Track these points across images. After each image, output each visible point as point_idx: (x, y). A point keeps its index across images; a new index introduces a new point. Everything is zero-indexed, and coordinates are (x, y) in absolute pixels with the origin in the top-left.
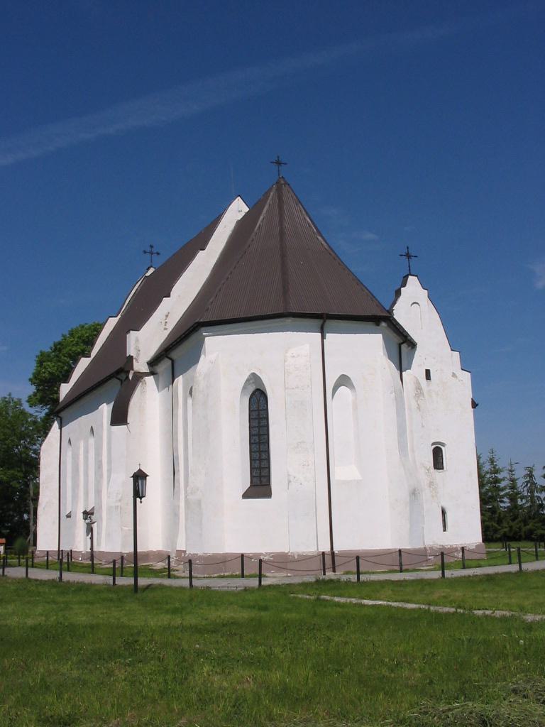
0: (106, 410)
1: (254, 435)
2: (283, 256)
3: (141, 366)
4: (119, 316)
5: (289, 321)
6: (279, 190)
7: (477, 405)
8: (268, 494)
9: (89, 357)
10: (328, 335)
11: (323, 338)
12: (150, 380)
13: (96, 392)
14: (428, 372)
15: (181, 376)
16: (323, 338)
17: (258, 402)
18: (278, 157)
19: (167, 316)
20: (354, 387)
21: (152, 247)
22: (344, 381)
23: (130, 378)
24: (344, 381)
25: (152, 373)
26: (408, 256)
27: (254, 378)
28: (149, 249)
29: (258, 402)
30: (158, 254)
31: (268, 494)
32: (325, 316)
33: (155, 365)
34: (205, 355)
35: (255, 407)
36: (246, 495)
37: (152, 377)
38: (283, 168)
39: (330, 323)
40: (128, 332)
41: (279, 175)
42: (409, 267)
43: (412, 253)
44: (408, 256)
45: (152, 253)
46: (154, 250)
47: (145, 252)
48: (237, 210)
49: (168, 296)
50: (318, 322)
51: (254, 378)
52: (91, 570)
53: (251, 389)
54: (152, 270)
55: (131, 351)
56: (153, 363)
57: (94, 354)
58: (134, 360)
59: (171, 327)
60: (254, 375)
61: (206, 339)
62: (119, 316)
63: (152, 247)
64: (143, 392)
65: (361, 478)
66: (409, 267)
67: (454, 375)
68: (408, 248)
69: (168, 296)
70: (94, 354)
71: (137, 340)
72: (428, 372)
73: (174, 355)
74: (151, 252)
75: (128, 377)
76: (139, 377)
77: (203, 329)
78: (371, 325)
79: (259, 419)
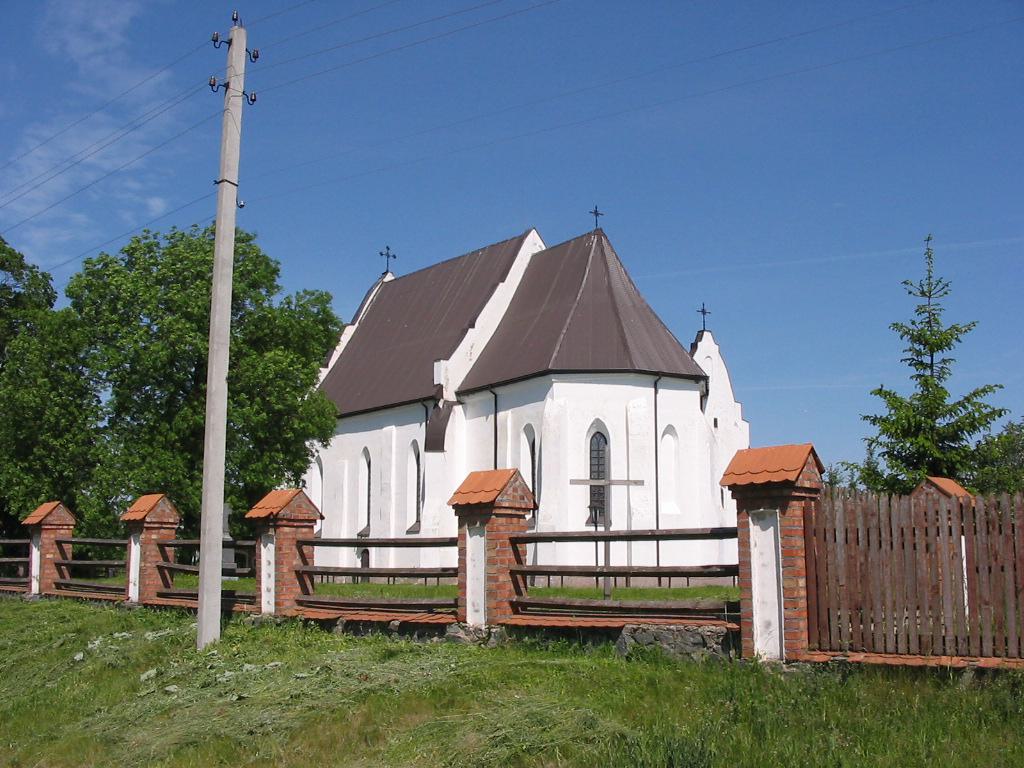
0: (418, 432)
2: (617, 314)
3: (449, 395)
4: (357, 324)
5: (632, 375)
6: (599, 242)
9: (326, 366)
10: (660, 391)
11: (656, 392)
12: (458, 409)
13: (388, 412)
14: (716, 420)
15: (509, 412)
16: (656, 392)
17: (599, 441)
20: (676, 435)
21: (388, 248)
22: (670, 430)
24: (670, 430)
25: (459, 402)
27: (598, 422)
28: (385, 251)
29: (599, 441)
30: (394, 257)
34: (552, 398)
35: (596, 448)
37: (460, 406)
38: (600, 218)
39: (664, 379)
40: (439, 360)
45: (388, 256)
48: (533, 245)
49: (473, 326)
50: (652, 379)
51: (598, 422)
53: (593, 432)
54: (389, 277)
56: (458, 394)
57: (331, 364)
60: (598, 420)
61: (554, 385)
62: (357, 324)
63: (388, 248)
64: (453, 421)
67: (736, 424)
70: (331, 364)
71: (447, 370)
72: (716, 420)
73: (499, 391)
74: (387, 254)
75: (436, 405)
76: (450, 406)
77: (552, 375)
78: (691, 383)
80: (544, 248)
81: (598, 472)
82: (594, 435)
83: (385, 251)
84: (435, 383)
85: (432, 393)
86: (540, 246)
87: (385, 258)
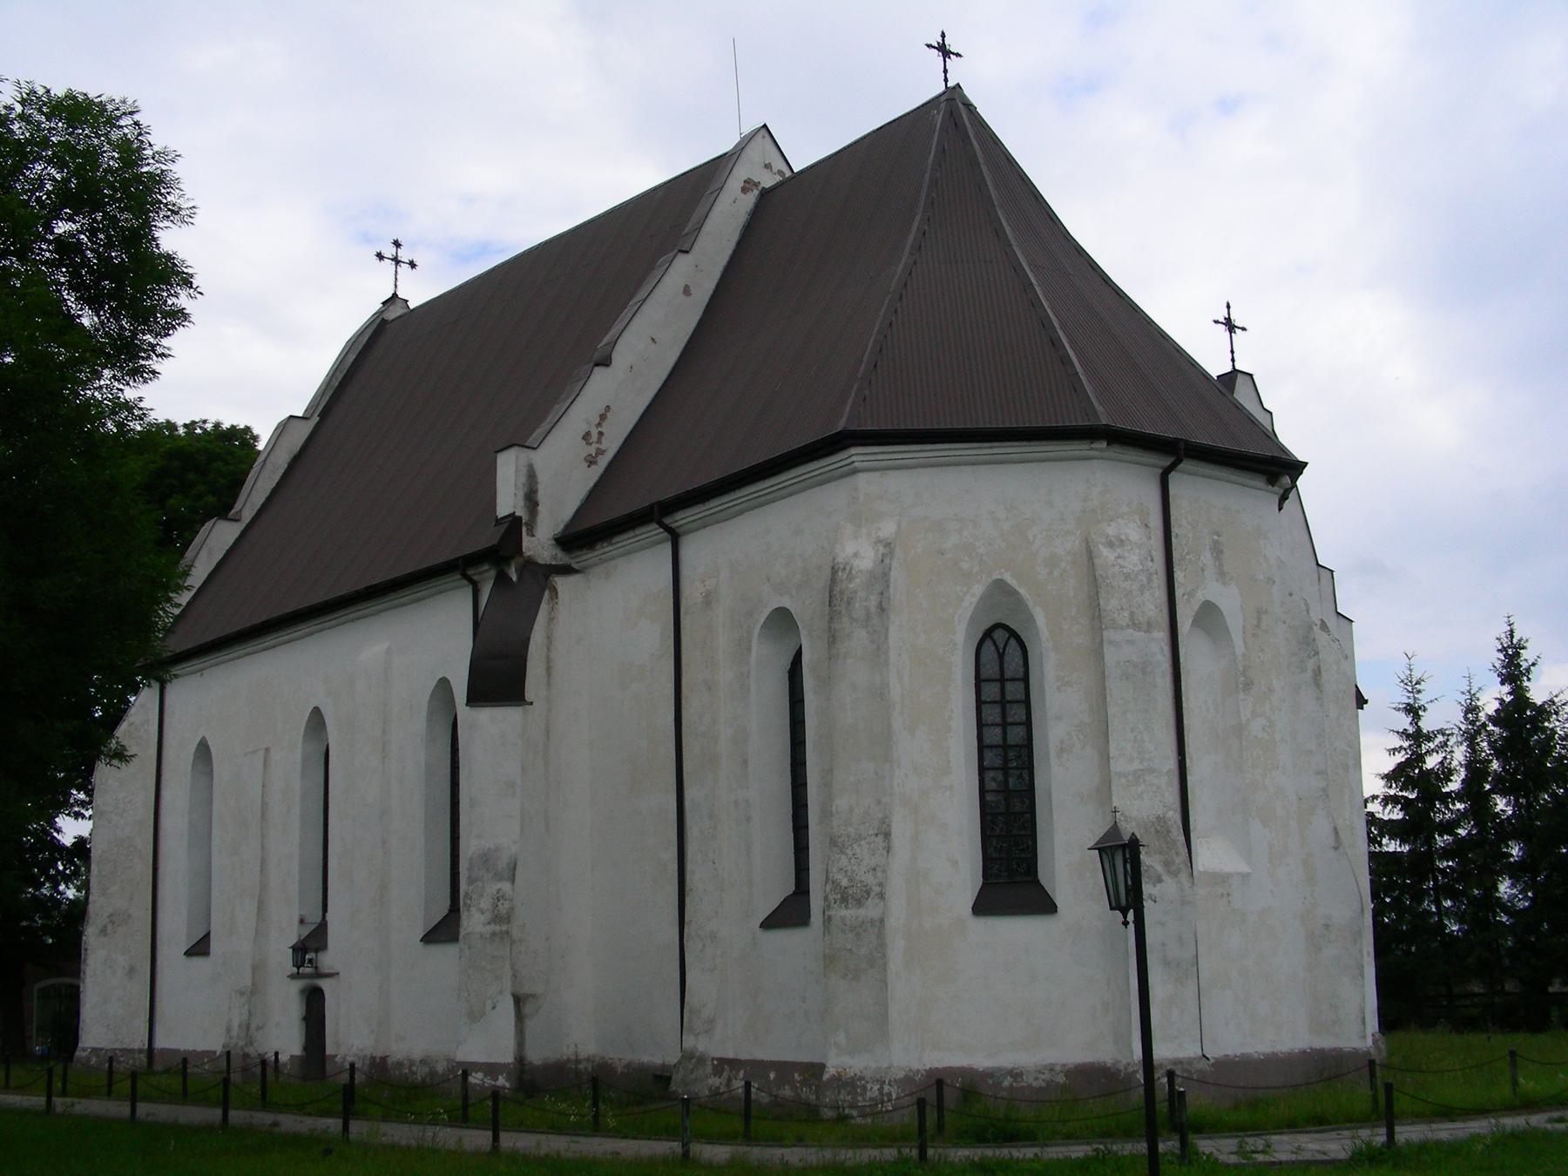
1: (991, 747)
3: (539, 544)
7: (1366, 702)
8: (1045, 905)
18: (943, 35)
19: (603, 417)
21: (397, 244)
23: (514, 579)
25: (566, 570)
26: (1230, 326)
28: (389, 251)
30: (412, 265)
31: (1045, 905)
32: (1182, 445)
33: (581, 547)
35: (991, 670)
36: (984, 906)
38: (952, 63)
39: (1186, 465)
41: (946, 80)
42: (1232, 352)
43: (1238, 321)
44: (1230, 326)
45: (397, 261)
46: (404, 255)
47: (380, 256)
49: (606, 362)
52: (739, 1125)
55: (508, 501)
58: (524, 529)
59: (612, 445)
60: (1000, 585)
63: (397, 244)
65: (1250, 871)
66: (1232, 352)
68: (1228, 307)
69: (606, 362)
71: (532, 476)
73: (680, 519)
77: (853, 450)
78: (1260, 482)
79: (1003, 703)
80: (788, 174)
81: (1005, 746)
82: (988, 634)
83: (389, 251)
84: (503, 510)
85: (488, 538)
86: (780, 173)
87: (389, 265)
